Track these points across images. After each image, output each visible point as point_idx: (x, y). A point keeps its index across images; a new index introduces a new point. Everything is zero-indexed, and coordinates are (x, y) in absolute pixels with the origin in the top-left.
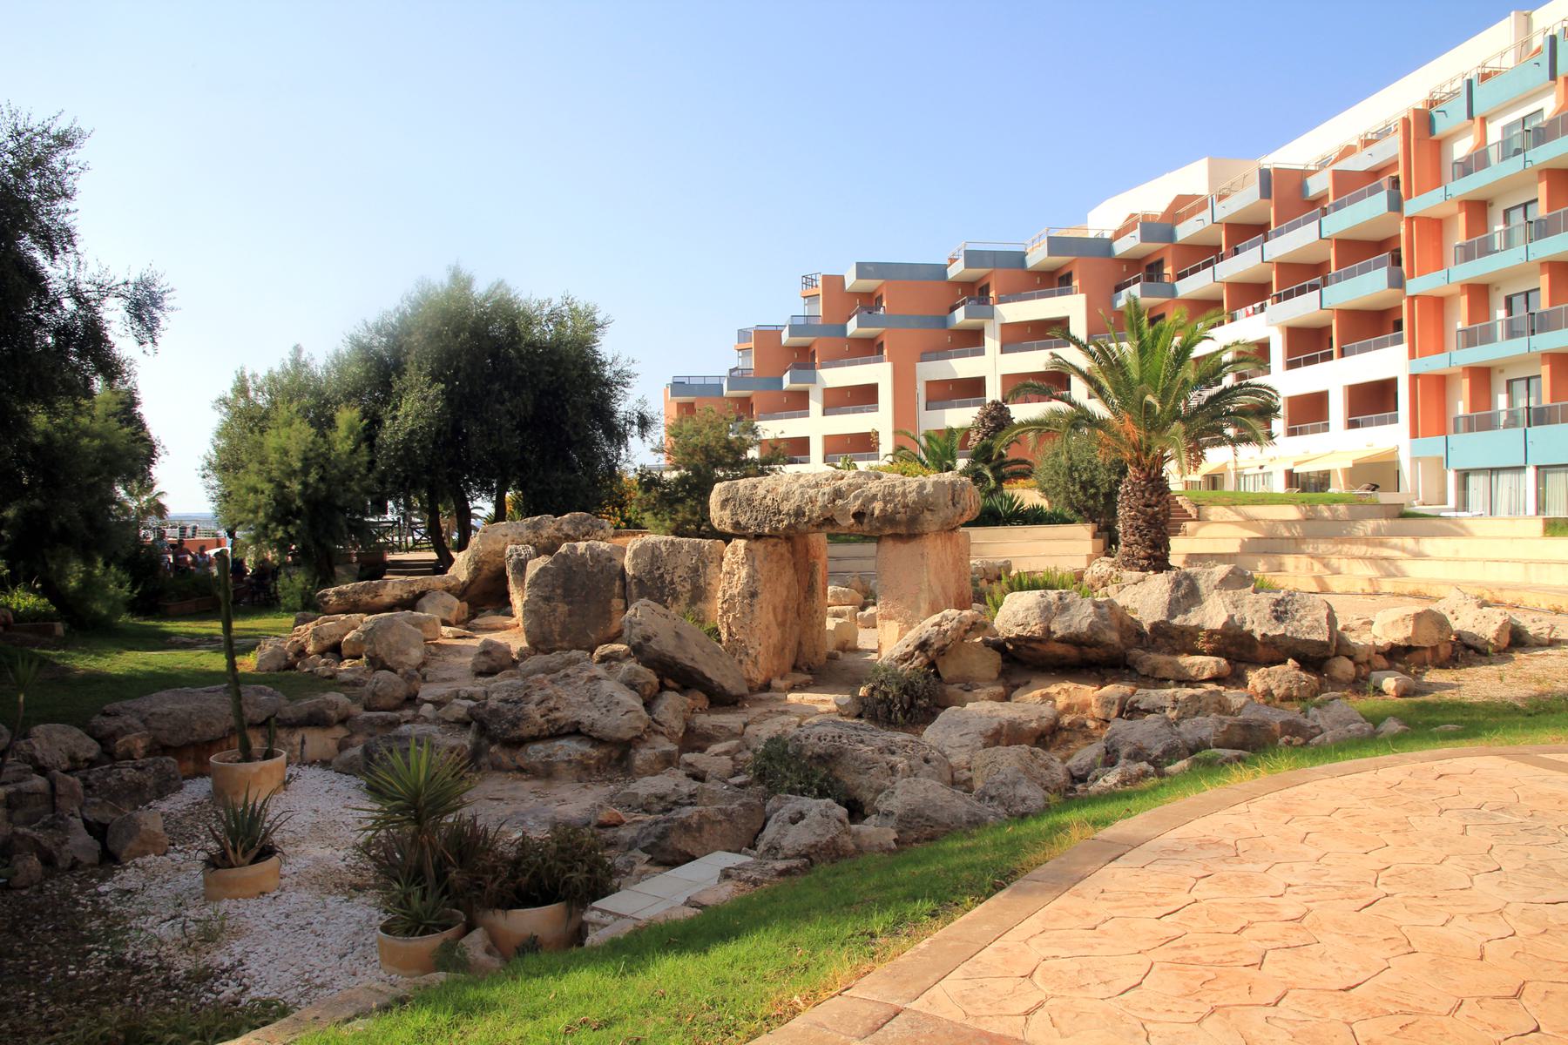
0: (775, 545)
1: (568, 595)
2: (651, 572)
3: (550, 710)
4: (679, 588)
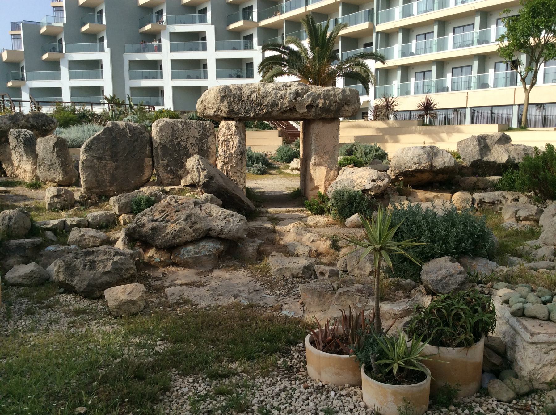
1: (114, 156)
2: (172, 141)
4: (190, 151)
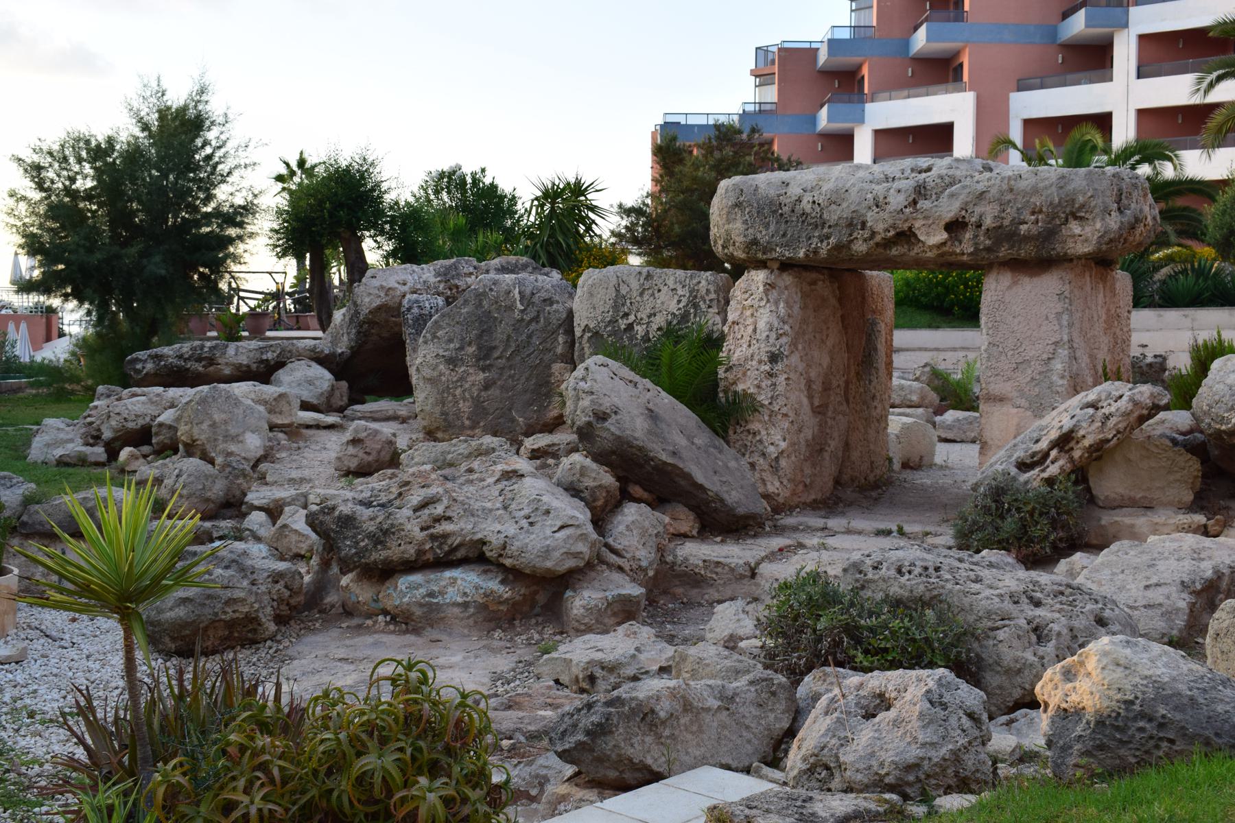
0: (814, 283)
2: (613, 321)
3: (438, 520)
